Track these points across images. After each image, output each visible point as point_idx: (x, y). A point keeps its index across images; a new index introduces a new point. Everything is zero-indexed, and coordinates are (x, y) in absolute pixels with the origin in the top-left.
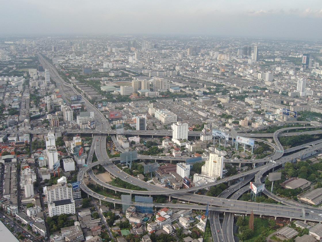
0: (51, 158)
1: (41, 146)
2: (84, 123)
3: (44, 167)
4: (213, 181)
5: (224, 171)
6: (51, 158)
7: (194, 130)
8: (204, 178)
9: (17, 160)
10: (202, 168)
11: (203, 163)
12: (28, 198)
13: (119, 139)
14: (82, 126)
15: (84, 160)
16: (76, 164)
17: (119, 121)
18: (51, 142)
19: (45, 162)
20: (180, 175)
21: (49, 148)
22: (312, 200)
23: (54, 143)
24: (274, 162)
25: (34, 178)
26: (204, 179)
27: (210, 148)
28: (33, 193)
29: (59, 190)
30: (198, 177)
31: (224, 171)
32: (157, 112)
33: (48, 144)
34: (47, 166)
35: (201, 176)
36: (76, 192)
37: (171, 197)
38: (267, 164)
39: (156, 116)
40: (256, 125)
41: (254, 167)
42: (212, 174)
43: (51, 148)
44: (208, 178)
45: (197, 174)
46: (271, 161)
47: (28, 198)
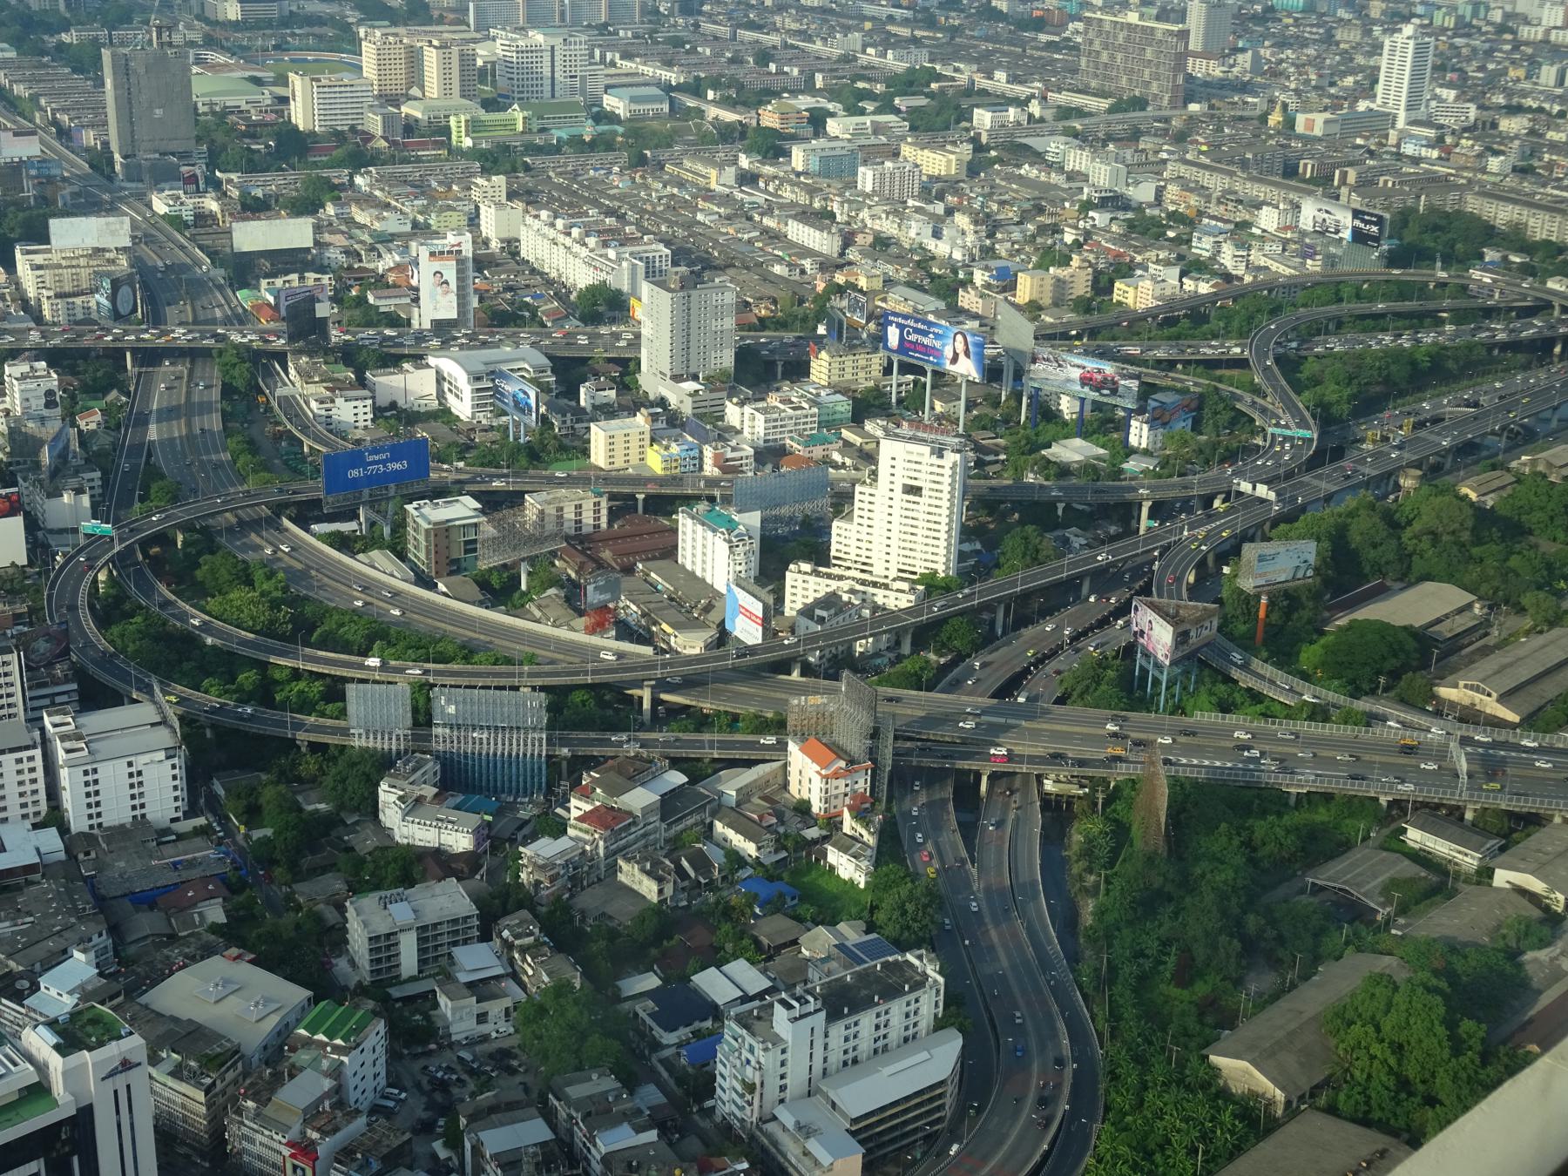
2: (68, 288)
4: (903, 604)
5: (967, 547)
8: (846, 585)
10: (834, 531)
11: (842, 502)
13: (306, 376)
16: (32, 526)
17: (294, 277)
20: (699, 573)
22: (1504, 698)
27: (869, 426)
30: (812, 579)
31: (967, 547)
32: (536, 224)
35: (829, 576)
36: (44, 685)
40: (1136, 295)
41: (1145, 523)
44: (875, 585)
45: (806, 567)
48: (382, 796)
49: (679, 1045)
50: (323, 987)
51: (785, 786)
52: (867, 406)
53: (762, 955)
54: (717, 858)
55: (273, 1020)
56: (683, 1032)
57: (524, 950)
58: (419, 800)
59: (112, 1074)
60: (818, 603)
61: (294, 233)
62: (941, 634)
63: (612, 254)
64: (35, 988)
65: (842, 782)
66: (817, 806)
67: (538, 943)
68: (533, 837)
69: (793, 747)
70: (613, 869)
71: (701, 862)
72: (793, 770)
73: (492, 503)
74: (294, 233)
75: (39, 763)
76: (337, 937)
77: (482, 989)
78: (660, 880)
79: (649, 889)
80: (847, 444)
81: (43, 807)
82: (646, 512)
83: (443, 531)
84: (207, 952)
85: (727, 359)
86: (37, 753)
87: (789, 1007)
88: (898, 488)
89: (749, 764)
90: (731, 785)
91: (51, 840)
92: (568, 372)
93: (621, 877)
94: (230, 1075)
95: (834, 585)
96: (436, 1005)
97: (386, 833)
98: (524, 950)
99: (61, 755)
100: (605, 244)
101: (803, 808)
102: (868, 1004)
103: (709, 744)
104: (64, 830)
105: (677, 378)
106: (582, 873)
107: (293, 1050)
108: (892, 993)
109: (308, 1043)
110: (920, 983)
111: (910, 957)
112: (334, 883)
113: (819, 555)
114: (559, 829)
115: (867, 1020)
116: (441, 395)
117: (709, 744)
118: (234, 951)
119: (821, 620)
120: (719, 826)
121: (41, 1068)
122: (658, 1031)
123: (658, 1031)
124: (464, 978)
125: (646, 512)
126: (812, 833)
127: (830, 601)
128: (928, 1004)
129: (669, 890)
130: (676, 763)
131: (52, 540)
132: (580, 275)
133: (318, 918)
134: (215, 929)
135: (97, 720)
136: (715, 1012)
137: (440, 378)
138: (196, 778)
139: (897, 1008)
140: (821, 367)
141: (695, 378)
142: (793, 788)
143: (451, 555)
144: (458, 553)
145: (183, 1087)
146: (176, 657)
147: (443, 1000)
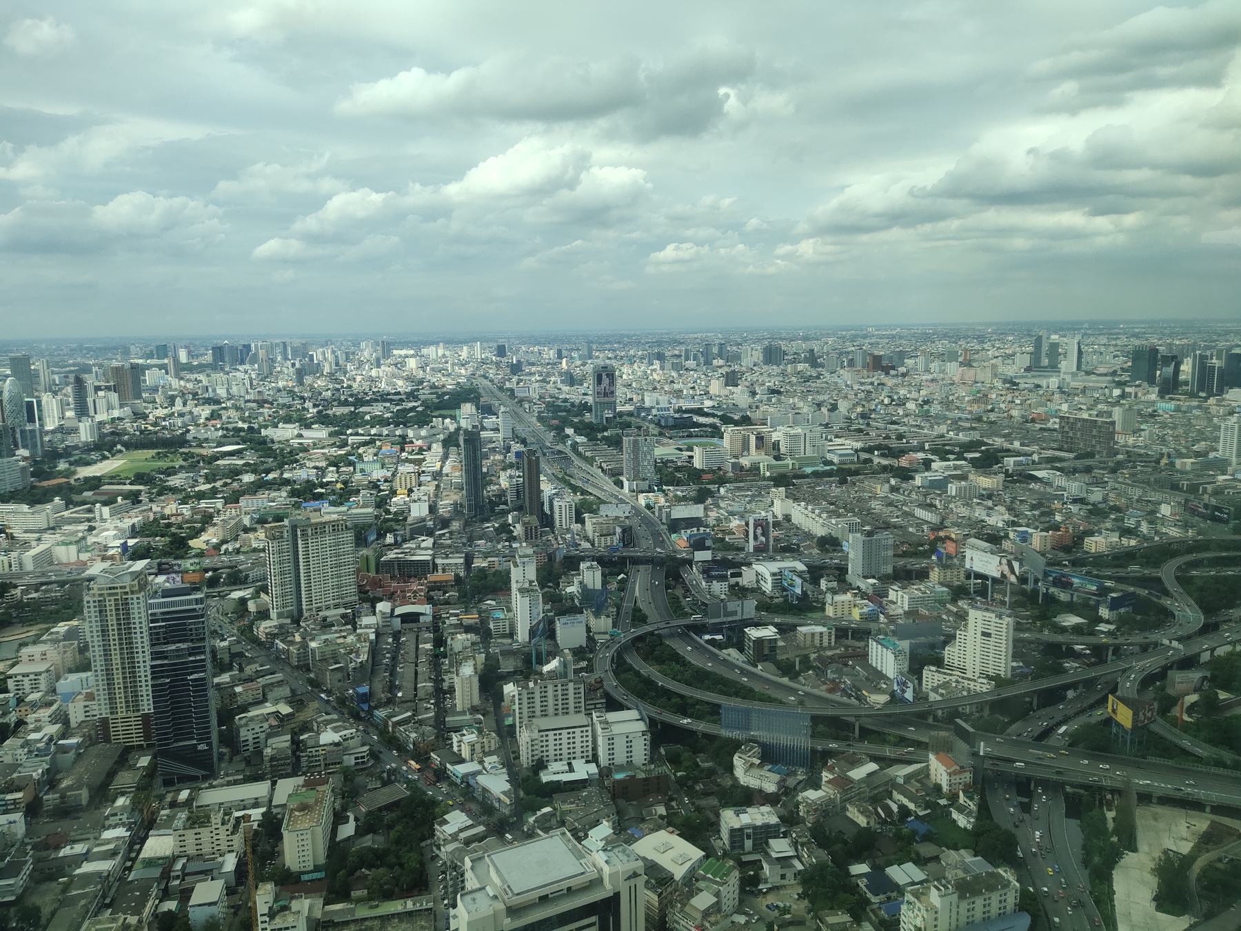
0: (522, 611)
1: (496, 584)
3: (504, 636)
4: (984, 690)
5: (1015, 664)
6: (522, 611)
7: (905, 555)
9: (434, 617)
11: (950, 639)
12: (463, 713)
14: (600, 542)
15: (610, 621)
18: (523, 573)
19: (507, 623)
21: (519, 585)
23: (532, 573)
24: (1175, 644)
25: (481, 658)
26: (957, 681)
27: (960, 603)
28: (476, 701)
29: (550, 688)
33: (515, 574)
34: (512, 635)
37: (861, 728)
38: (1150, 650)
39: (795, 520)
40: (1097, 544)
42: (977, 671)
43: (527, 585)
44: (969, 679)
45: (934, 668)
46: (1166, 642)
47: (463, 713)
48: (735, 762)
49: (881, 903)
50: (709, 852)
51: (928, 776)
52: (959, 592)
53: (920, 862)
54: (895, 808)
55: (688, 865)
56: (882, 897)
57: (803, 845)
58: (752, 765)
59: (629, 878)
60: (939, 686)
61: (696, 511)
62: (1003, 708)
63: (833, 521)
64: (586, 836)
65: (957, 777)
66: (945, 788)
67: (809, 842)
68: (805, 789)
69: (932, 757)
70: (845, 809)
71: (887, 809)
72: (932, 768)
73: (782, 629)
74: (696, 511)
75: (590, 733)
76: (714, 826)
77: (784, 861)
78: (868, 817)
79: (862, 821)
80: (950, 611)
81: (590, 753)
82: (852, 637)
83: (759, 642)
84: (658, 828)
85: (889, 570)
86: (589, 729)
87: (939, 889)
88: (979, 634)
89: (909, 763)
90: (901, 772)
91: (593, 768)
92: (814, 574)
93: (849, 814)
94: (669, 890)
95: (948, 678)
96: (762, 868)
97: (736, 779)
98: (803, 845)
99: (599, 731)
100: (830, 517)
101: (938, 788)
102: (980, 893)
103: (888, 751)
104: (598, 766)
105: (866, 577)
106: (827, 811)
107: (697, 880)
108: (991, 888)
109: (704, 878)
110: (1006, 885)
111: (1000, 871)
112: (714, 801)
113: (939, 662)
114: (817, 786)
115: (979, 902)
116: (758, 581)
117: (888, 751)
118: (671, 829)
119: (942, 695)
120: (895, 793)
121: (600, 871)
122: (869, 895)
123: (869, 895)
124: (774, 855)
125: (852, 637)
126: (943, 802)
127: (945, 685)
128: (1011, 899)
129: (872, 824)
130: (874, 759)
131: (596, 637)
132: (820, 531)
133: (708, 819)
134: (661, 817)
135: (612, 716)
136: (900, 890)
137: (758, 574)
138: (654, 744)
139: (995, 898)
140: (935, 575)
141: (874, 577)
142: (933, 777)
143: (763, 651)
144: (766, 652)
145: (649, 893)
146: (646, 691)
147: (765, 865)
